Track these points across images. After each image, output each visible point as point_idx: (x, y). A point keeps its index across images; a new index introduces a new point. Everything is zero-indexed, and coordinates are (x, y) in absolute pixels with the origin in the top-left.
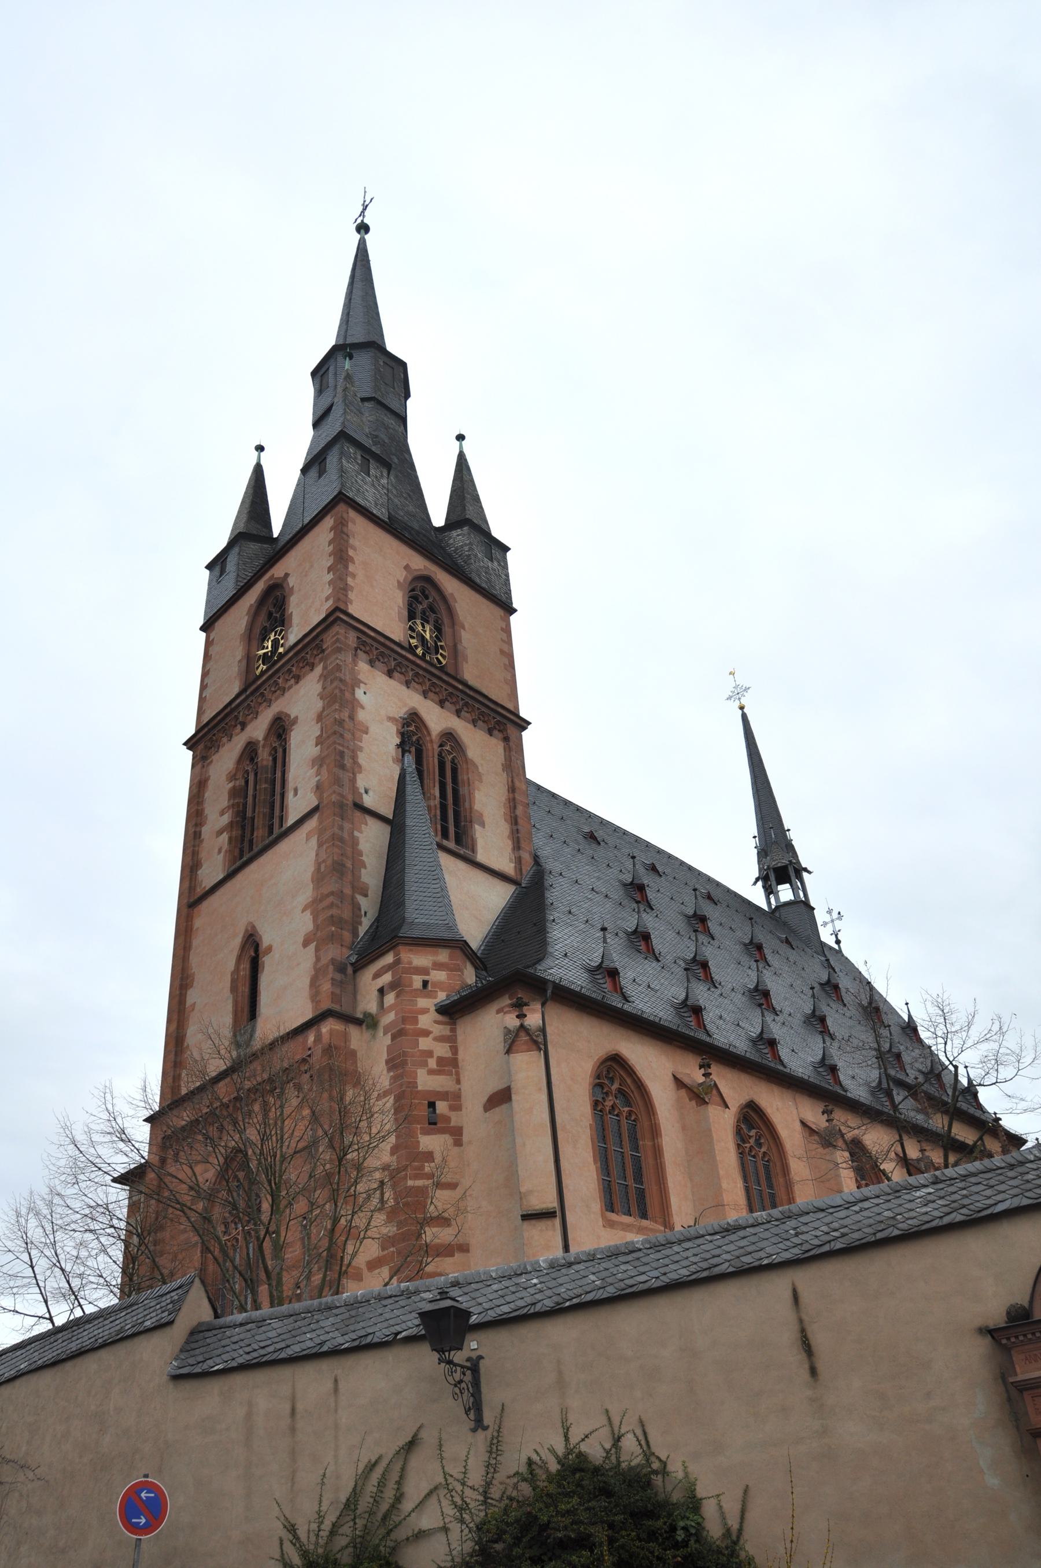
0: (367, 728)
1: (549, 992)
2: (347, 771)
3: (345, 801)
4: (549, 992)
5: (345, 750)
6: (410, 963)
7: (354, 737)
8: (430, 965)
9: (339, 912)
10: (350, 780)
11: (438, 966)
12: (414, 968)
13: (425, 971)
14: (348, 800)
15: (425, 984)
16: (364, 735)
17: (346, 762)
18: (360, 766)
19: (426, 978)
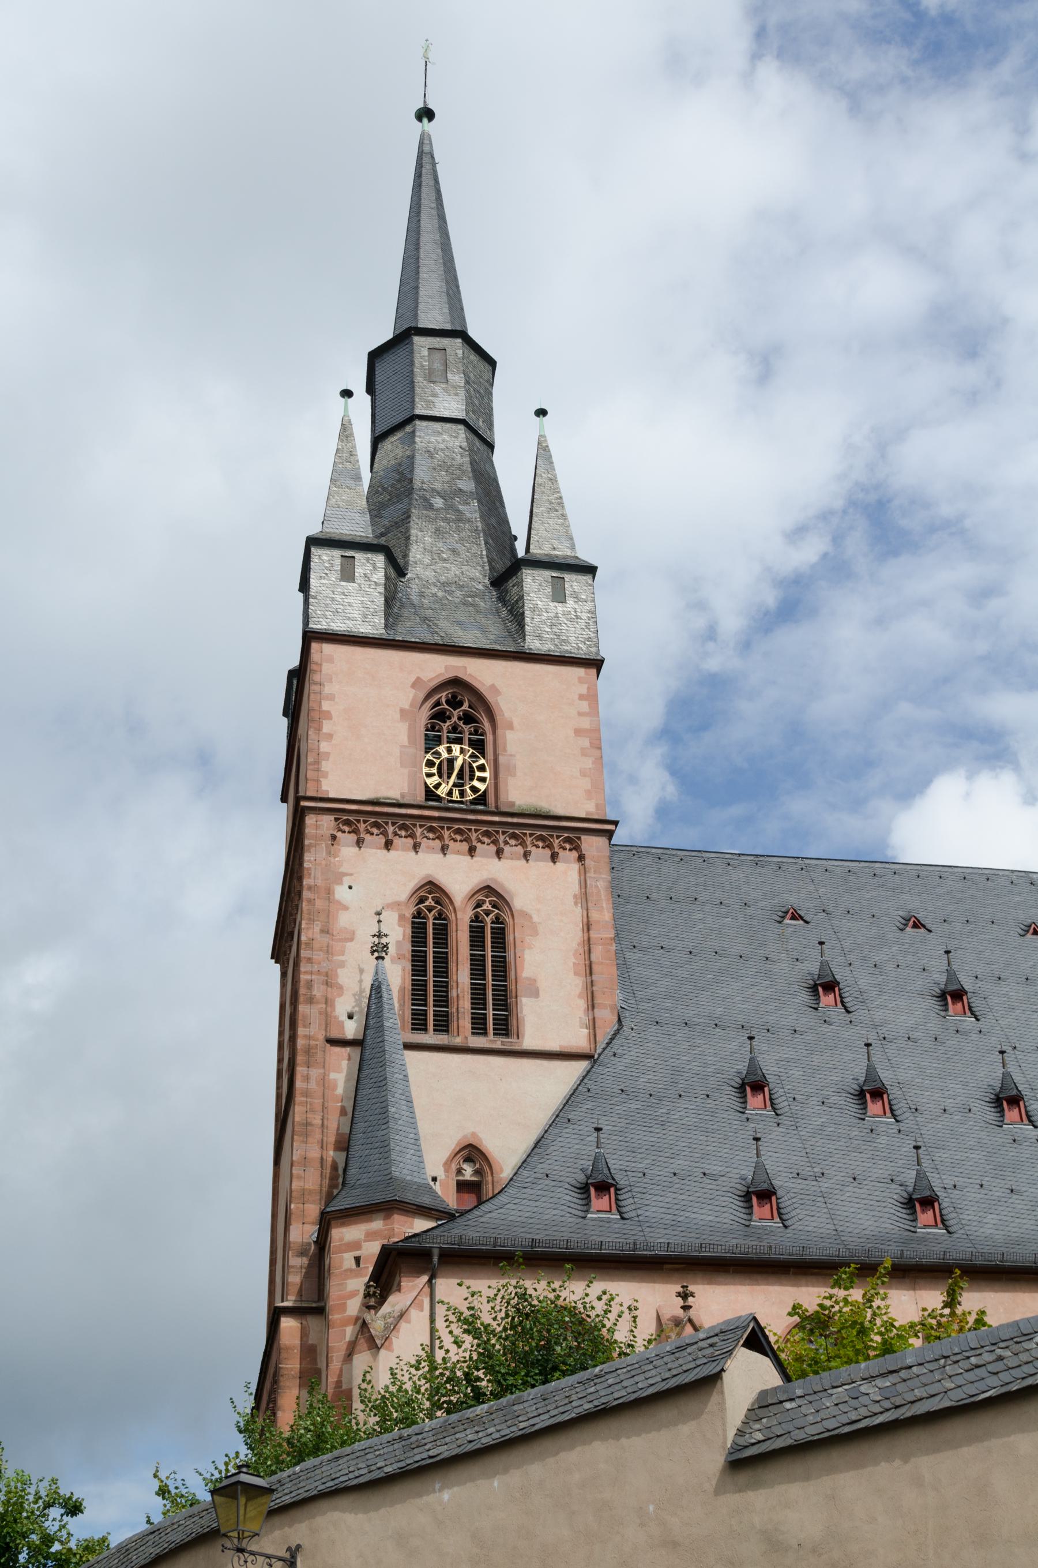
0: (354, 933)
1: (435, 1259)
2: (318, 1003)
3: (312, 1043)
4: (435, 1259)
5: (314, 977)
6: (341, 1239)
7: (328, 951)
8: (363, 1237)
9: (302, 1184)
10: (320, 1013)
11: (370, 1236)
12: (344, 1244)
13: (356, 1245)
14: (317, 1040)
15: (358, 1260)
16: (348, 944)
17: (315, 992)
18: (340, 988)
19: (357, 1253)
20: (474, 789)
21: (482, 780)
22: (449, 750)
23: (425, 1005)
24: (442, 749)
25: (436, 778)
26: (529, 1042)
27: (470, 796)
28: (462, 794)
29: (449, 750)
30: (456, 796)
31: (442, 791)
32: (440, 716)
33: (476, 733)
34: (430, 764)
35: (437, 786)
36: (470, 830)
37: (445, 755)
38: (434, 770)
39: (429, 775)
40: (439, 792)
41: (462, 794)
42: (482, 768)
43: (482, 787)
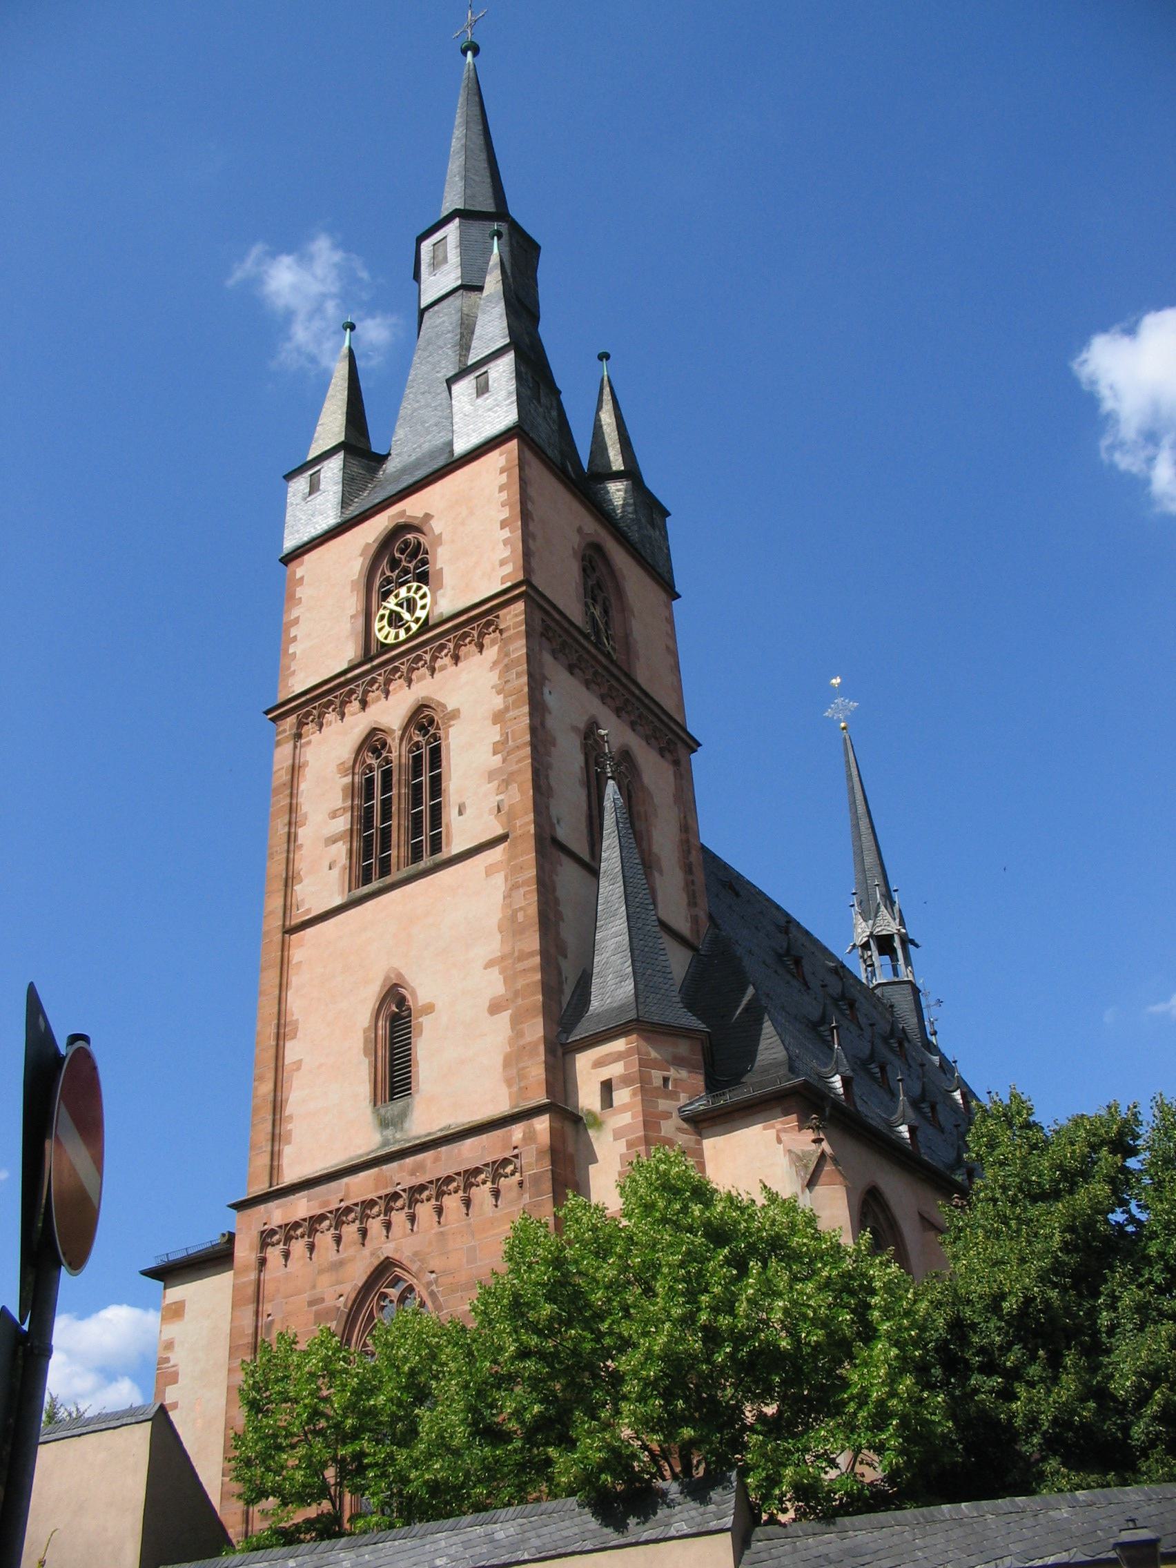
27: (415, 627)
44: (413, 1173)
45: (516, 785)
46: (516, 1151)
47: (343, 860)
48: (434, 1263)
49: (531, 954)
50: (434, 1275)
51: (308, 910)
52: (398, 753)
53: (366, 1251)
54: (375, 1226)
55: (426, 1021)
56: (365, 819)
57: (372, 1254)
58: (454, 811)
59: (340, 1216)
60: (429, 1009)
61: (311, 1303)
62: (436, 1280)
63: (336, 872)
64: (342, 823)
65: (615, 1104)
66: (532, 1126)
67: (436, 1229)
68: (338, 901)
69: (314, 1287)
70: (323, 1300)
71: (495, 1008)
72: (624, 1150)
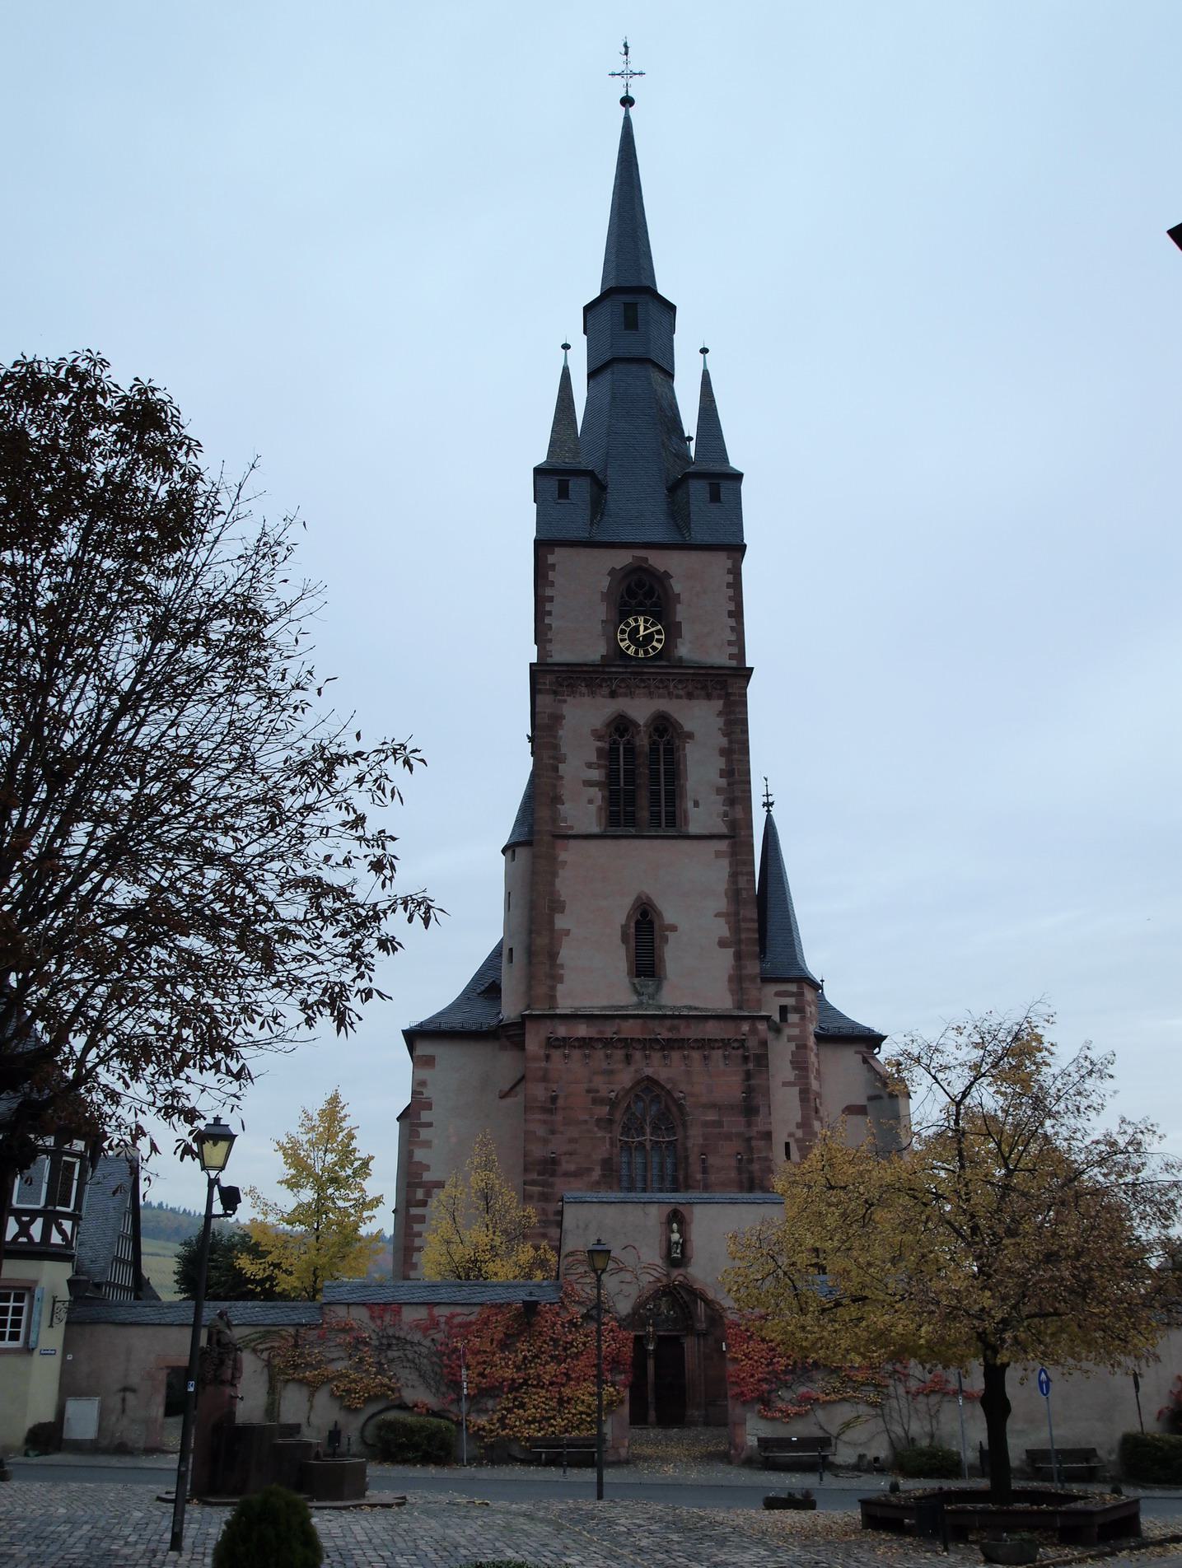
20: (654, 648)
21: (659, 641)
22: (636, 621)
23: (619, 806)
24: (631, 620)
25: (627, 641)
26: (693, 829)
27: (652, 653)
28: (646, 652)
29: (636, 621)
30: (641, 654)
31: (631, 651)
32: (630, 593)
33: (655, 605)
34: (623, 632)
35: (628, 648)
36: (649, 679)
37: (633, 624)
38: (626, 636)
39: (622, 640)
40: (629, 652)
41: (646, 652)
42: (659, 632)
43: (660, 646)
44: (670, 1030)
45: (740, 807)
46: (744, 1037)
47: (599, 802)
48: (683, 1087)
49: (752, 920)
50: (682, 1095)
51: (571, 828)
52: (643, 741)
53: (632, 1069)
54: (638, 1055)
55: (671, 935)
56: (612, 777)
57: (636, 1071)
58: (690, 804)
59: (608, 1043)
60: (674, 928)
61: (589, 1091)
62: (684, 1098)
63: (593, 808)
64: (596, 775)
65: (789, 1021)
66: (754, 1025)
67: (683, 1068)
68: (595, 829)
69: (590, 1081)
70: (598, 1091)
71: (722, 944)
72: (794, 1049)
